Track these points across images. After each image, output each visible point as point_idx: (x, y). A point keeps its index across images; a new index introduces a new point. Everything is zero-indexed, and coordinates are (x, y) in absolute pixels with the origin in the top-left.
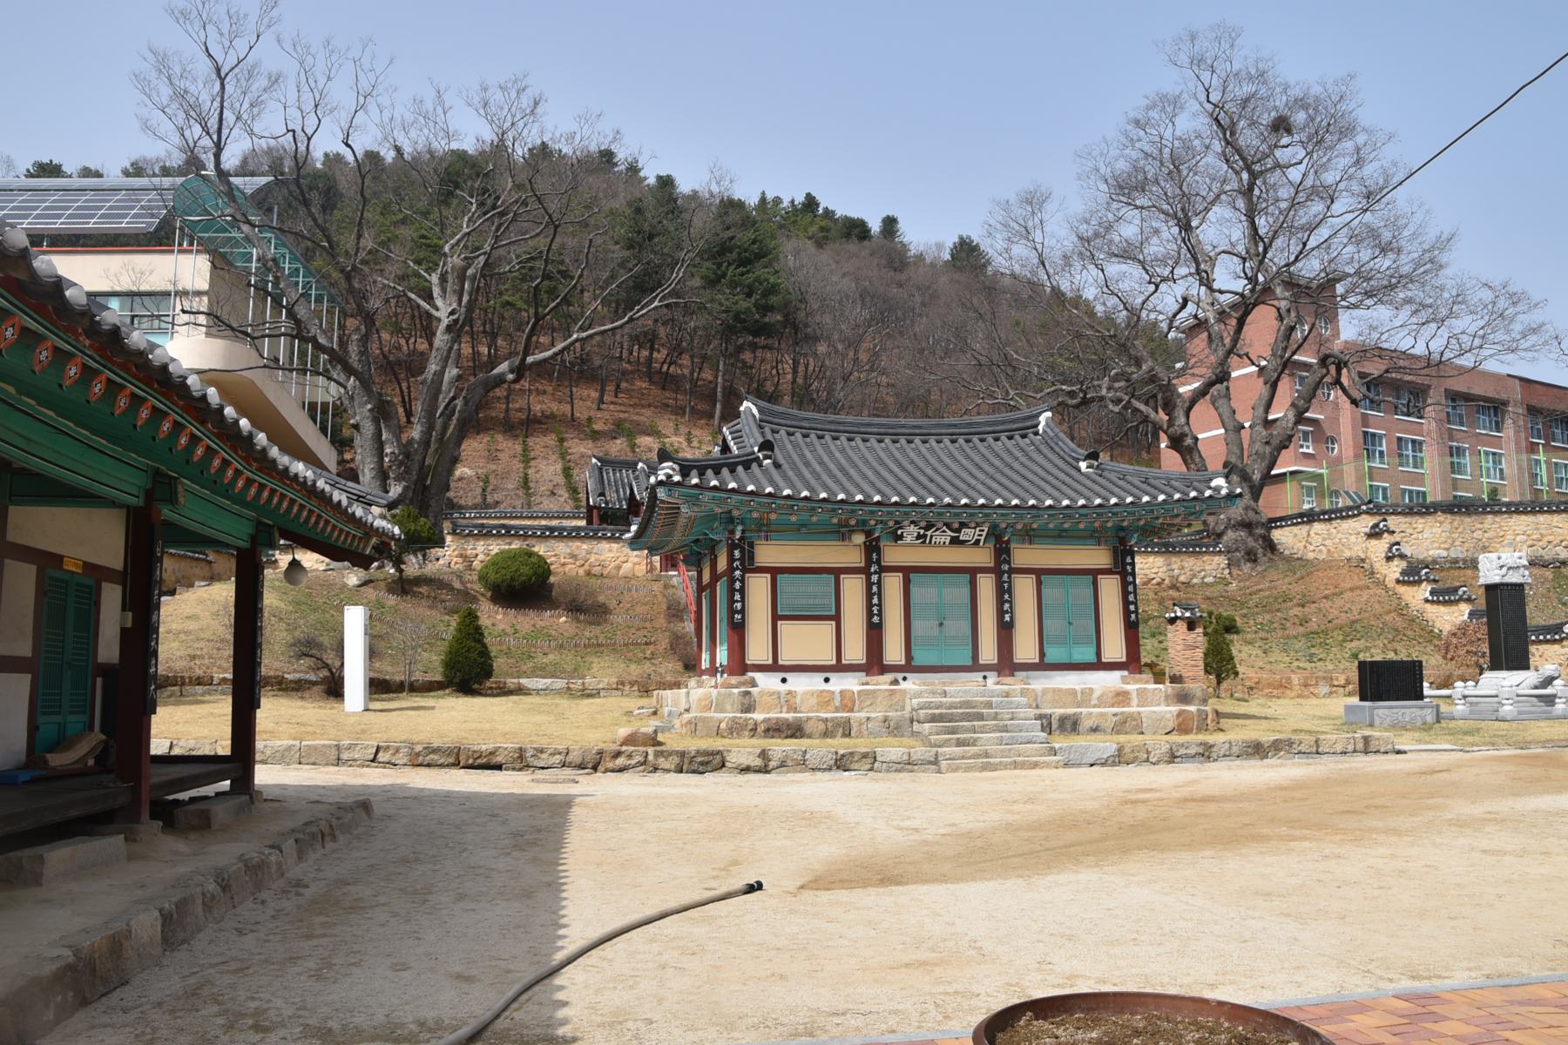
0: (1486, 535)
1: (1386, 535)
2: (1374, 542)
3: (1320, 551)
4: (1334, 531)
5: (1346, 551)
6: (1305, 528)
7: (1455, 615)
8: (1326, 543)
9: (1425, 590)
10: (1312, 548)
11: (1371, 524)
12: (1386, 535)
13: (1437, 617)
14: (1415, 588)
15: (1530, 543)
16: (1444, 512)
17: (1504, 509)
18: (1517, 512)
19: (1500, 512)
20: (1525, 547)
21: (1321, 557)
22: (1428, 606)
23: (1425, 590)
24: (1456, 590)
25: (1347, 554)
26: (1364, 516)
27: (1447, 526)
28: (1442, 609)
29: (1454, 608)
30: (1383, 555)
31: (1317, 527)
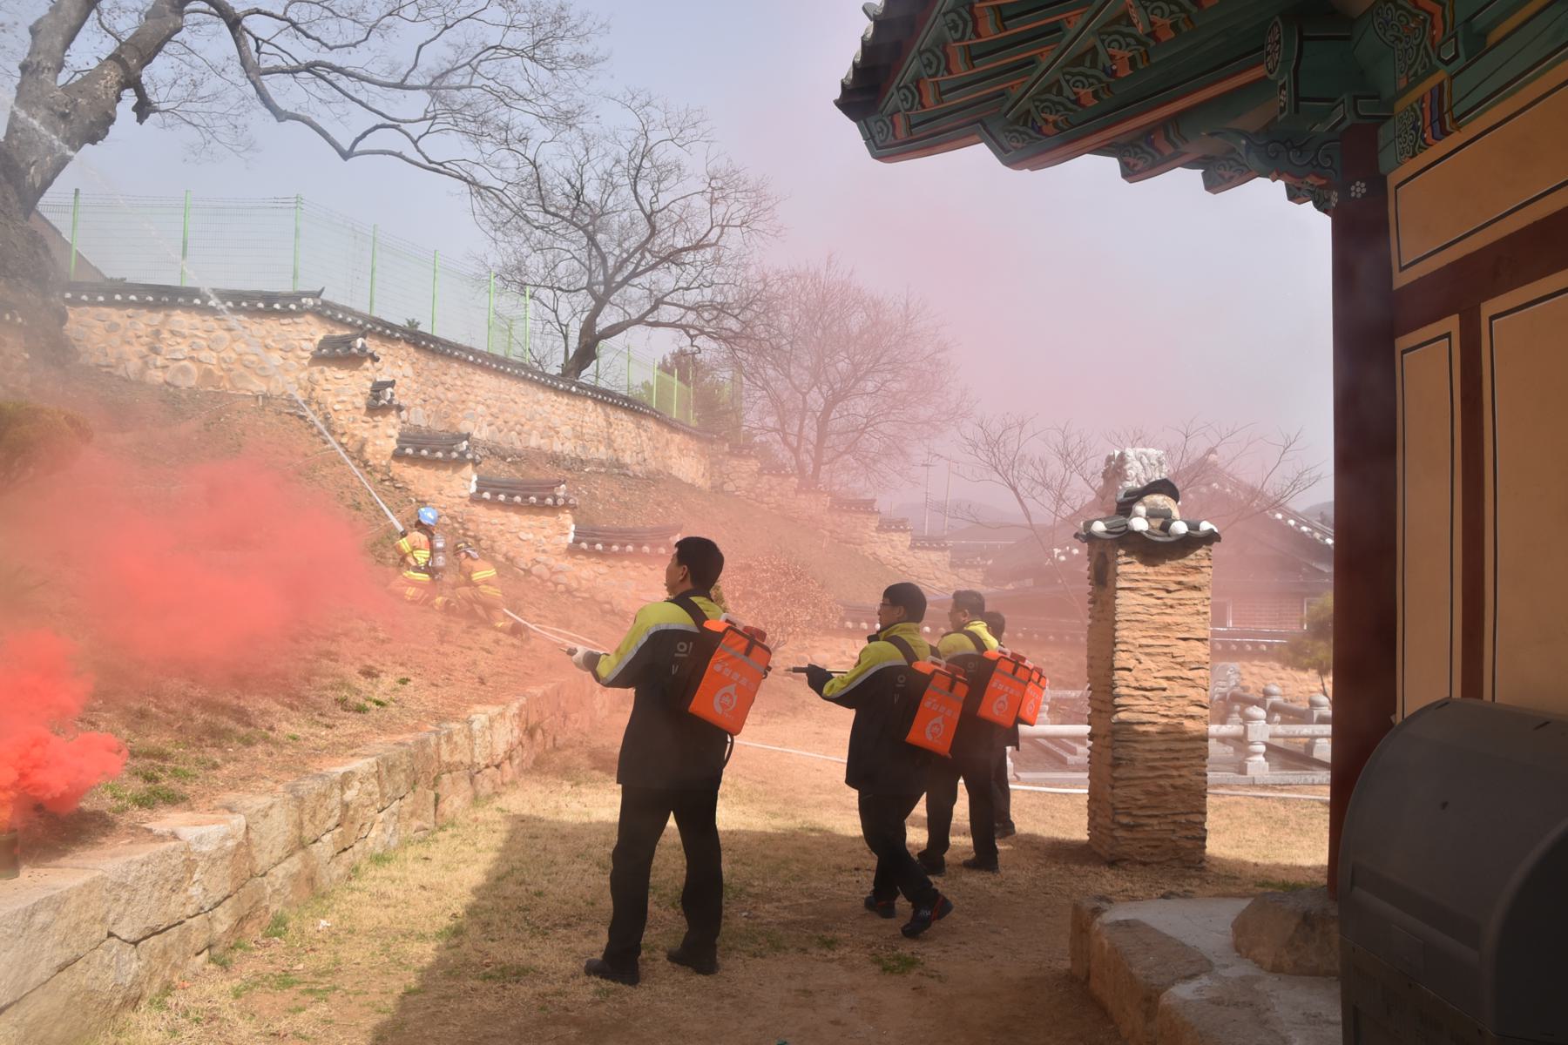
0: (450, 395)
1: (368, 364)
2: (332, 372)
3: (185, 371)
4: (226, 335)
5: (255, 379)
6: (158, 317)
7: (548, 532)
8: (203, 355)
9: (467, 481)
10: (160, 361)
11: (319, 337)
12: (368, 364)
13: (502, 533)
14: (445, 474)
15: (489, 418)
16: (407, 342)
17: (471, 358)
18: (481, 366)
19: (466, 361)
20: (485, 425)
21: (185, 383)
22: (480, 511)
23: (467, 481)
24: (551, 486)
25: (258, 386)
26: (309, 318)
27: (408, 370)
28: (515, 519)
29: (546, 520)
30: (361, 402)
31: (180, 319)
